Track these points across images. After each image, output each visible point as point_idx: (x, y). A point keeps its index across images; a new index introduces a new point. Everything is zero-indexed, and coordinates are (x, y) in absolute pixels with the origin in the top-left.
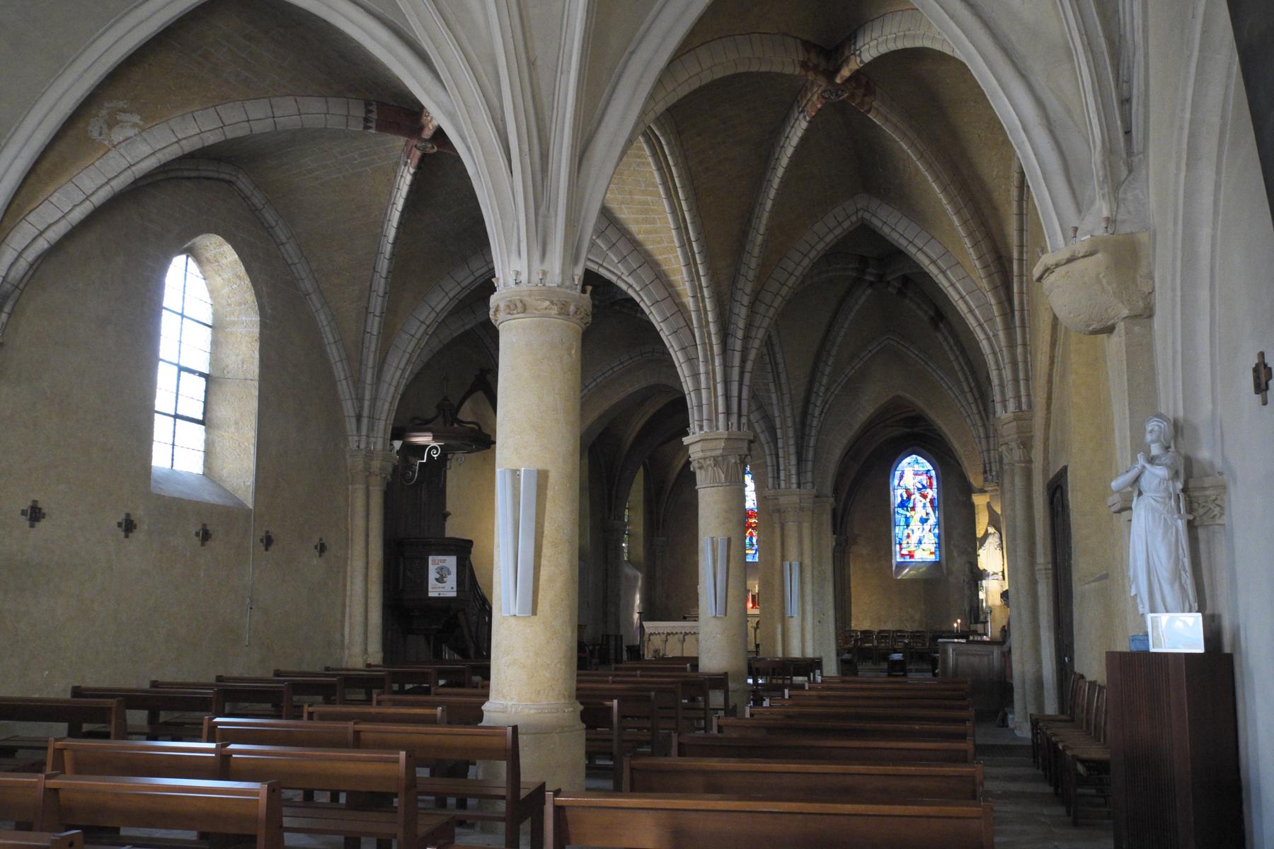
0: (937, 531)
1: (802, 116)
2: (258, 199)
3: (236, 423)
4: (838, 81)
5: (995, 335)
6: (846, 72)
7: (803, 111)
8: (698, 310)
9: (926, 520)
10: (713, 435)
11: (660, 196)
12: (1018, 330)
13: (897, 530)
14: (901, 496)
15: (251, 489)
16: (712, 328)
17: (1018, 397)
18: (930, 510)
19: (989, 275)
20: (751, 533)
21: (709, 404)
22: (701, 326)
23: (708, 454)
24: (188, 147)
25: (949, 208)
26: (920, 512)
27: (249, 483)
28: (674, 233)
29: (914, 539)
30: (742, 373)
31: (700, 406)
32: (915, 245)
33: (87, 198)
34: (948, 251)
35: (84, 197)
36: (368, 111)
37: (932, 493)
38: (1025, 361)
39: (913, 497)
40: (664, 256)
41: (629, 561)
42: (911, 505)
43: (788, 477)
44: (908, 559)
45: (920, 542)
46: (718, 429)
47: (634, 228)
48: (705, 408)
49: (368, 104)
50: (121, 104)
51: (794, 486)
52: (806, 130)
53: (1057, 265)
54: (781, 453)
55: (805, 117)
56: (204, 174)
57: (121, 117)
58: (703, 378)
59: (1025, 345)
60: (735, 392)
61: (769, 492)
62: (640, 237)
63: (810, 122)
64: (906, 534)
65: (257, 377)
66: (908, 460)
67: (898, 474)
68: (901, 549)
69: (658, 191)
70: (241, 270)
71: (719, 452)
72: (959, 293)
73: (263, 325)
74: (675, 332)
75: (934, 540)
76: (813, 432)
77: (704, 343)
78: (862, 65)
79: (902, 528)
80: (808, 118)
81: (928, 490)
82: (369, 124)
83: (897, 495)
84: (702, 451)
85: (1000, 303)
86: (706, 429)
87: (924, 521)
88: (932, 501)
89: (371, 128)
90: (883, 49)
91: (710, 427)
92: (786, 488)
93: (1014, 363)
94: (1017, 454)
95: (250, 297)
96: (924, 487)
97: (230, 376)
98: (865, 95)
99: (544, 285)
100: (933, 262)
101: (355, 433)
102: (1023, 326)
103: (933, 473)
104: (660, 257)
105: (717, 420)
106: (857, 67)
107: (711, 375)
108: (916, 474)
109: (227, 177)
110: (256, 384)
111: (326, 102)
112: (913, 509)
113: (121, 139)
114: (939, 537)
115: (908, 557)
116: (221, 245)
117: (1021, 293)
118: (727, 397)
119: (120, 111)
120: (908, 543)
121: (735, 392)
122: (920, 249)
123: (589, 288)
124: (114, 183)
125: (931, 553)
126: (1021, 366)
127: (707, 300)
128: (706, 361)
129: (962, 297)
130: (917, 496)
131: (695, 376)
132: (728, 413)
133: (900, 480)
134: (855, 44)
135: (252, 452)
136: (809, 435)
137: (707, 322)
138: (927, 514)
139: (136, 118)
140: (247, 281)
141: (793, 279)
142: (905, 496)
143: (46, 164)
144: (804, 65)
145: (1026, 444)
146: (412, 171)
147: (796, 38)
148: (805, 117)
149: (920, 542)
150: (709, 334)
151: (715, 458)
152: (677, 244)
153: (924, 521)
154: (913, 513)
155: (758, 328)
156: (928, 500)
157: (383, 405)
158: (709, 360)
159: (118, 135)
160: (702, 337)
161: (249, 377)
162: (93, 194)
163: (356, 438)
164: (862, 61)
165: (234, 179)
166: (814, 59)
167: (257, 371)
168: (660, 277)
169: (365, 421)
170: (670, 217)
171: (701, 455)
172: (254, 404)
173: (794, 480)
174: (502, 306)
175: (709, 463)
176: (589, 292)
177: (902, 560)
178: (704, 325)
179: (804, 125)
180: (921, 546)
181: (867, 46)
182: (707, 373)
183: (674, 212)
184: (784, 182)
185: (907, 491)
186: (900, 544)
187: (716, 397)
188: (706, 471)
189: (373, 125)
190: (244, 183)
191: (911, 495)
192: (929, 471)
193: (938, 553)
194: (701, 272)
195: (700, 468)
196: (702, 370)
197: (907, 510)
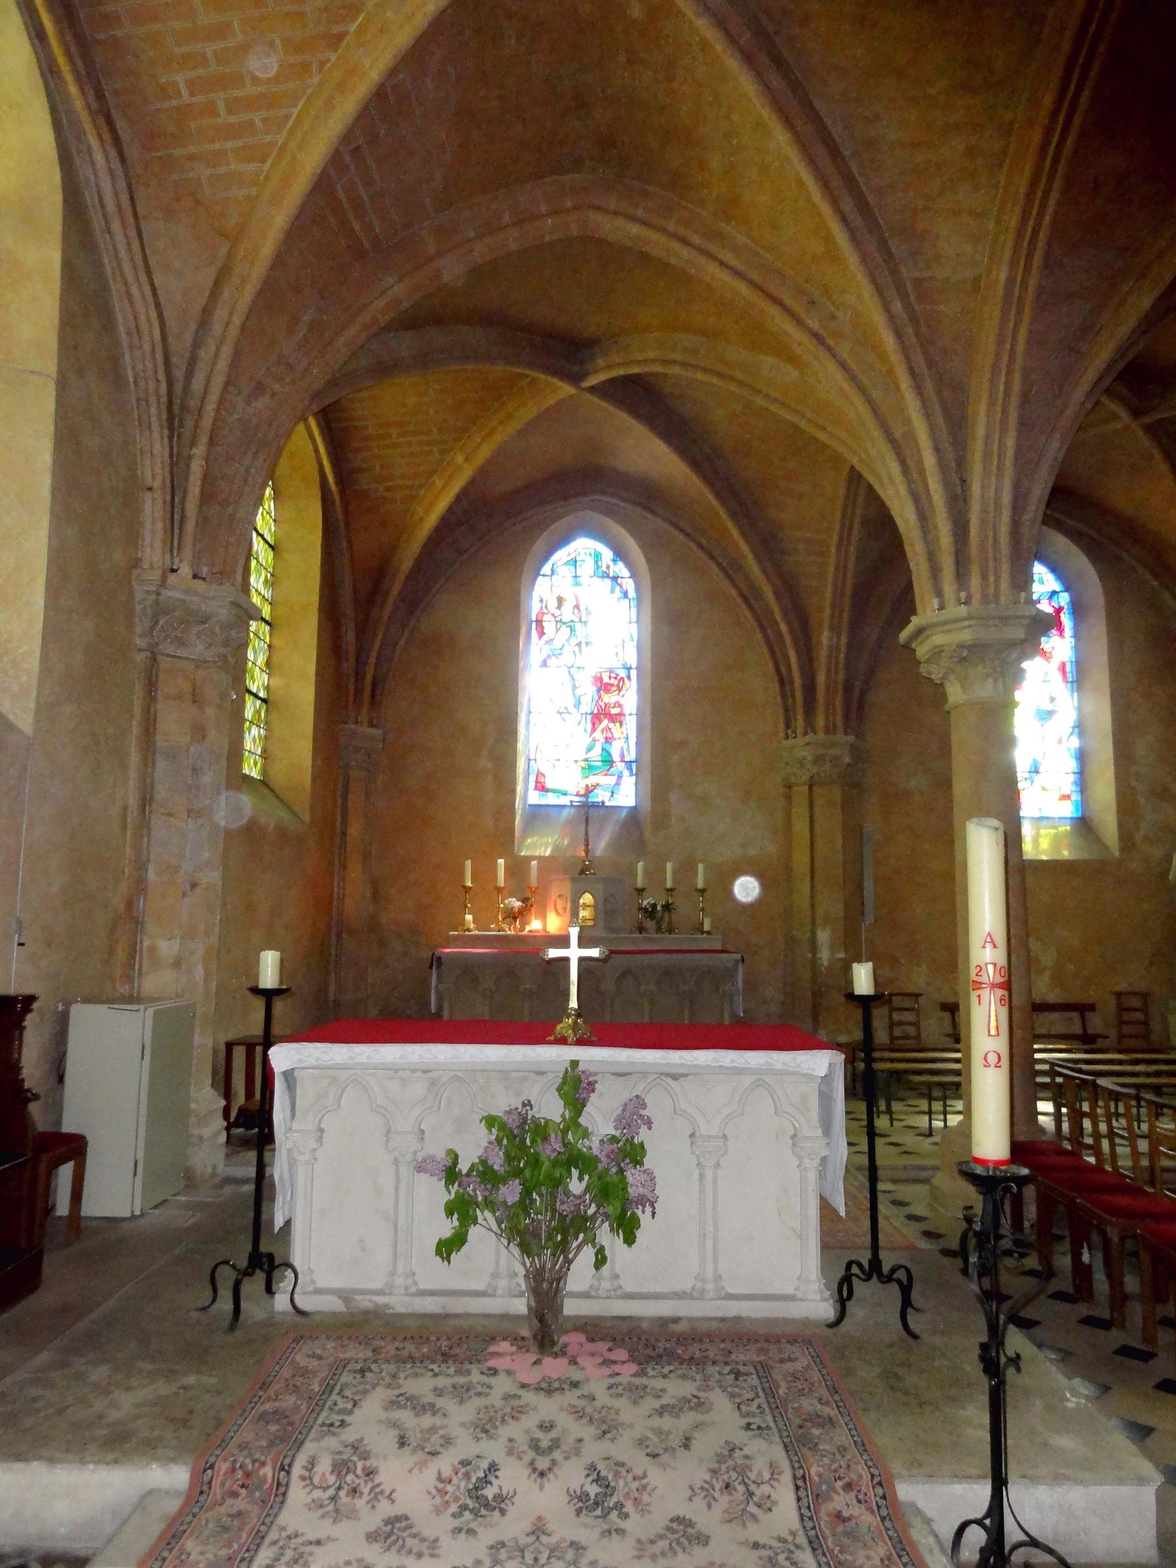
88: (1063, 667)
125: (1066, 797)
138: (1052, 700)
180: (1037, 778)
192: (1054, 593)
193: (1076, 797)
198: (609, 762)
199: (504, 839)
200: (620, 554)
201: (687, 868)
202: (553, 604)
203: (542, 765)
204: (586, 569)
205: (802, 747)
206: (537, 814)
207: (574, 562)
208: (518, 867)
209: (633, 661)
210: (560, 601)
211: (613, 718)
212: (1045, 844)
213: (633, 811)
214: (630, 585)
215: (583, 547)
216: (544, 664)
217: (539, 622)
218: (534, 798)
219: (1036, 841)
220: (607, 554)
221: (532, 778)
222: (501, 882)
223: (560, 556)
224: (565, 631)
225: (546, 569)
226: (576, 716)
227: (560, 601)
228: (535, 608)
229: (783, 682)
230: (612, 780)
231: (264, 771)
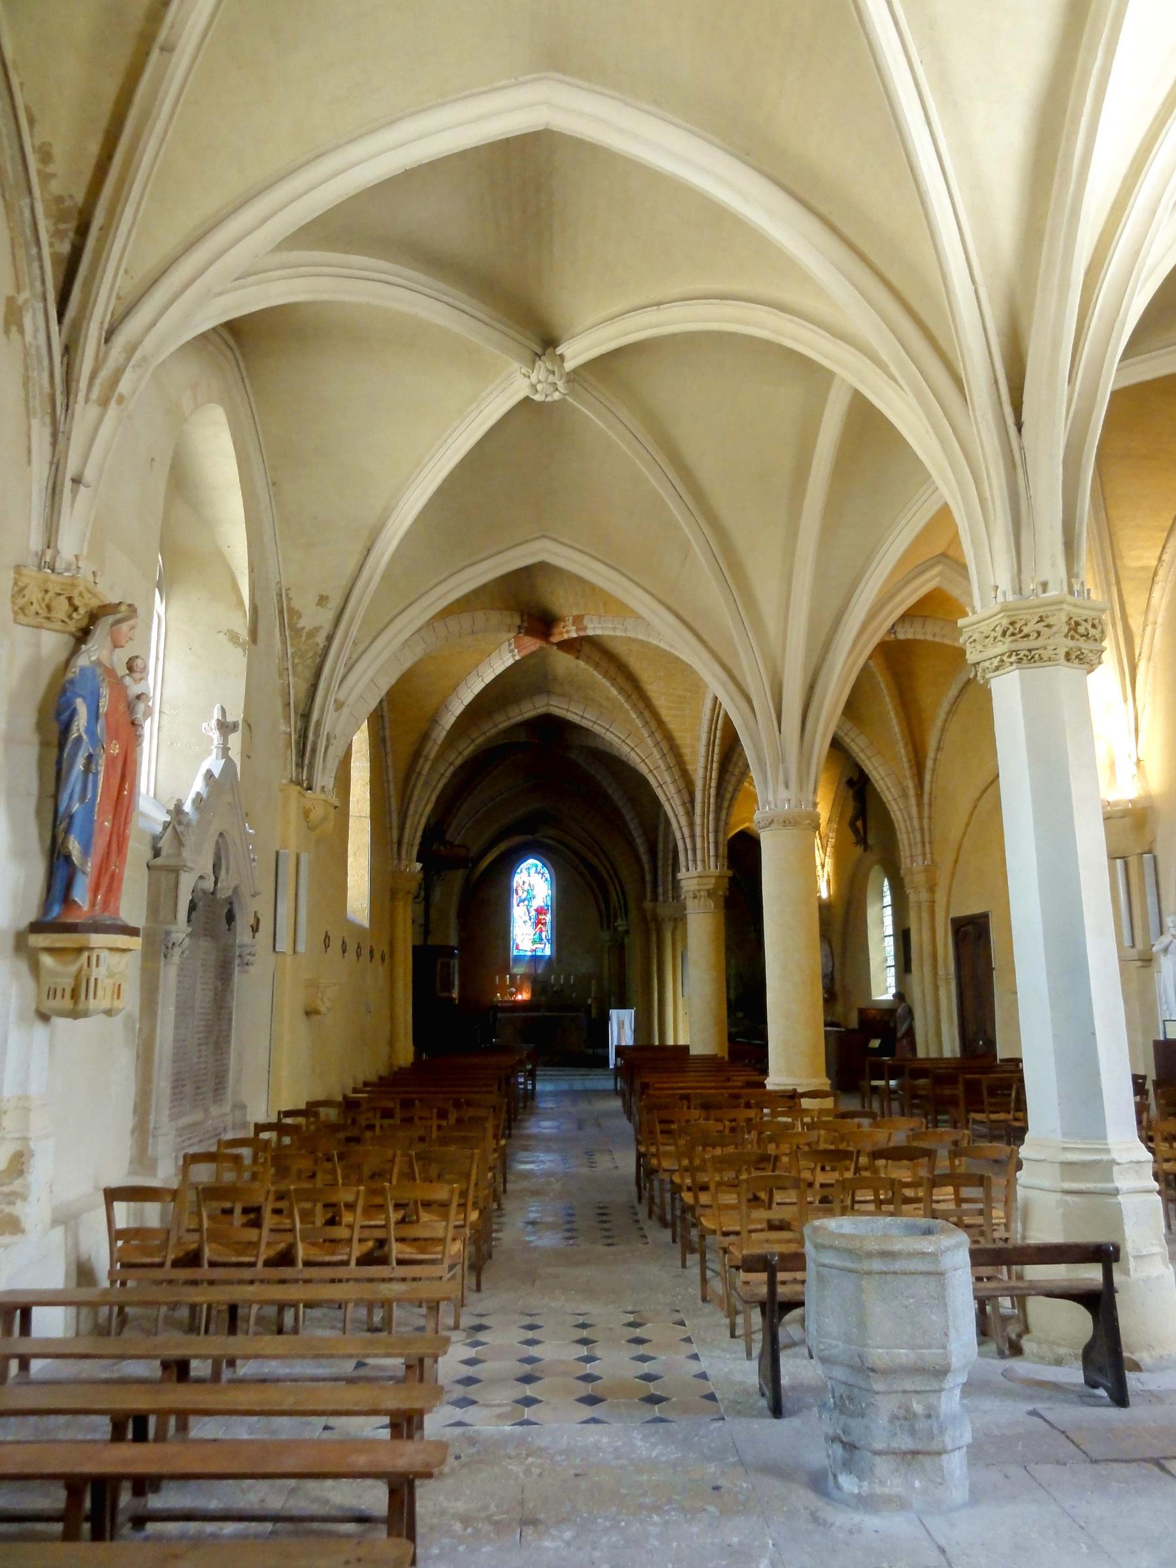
5: (907, 808)
10: (707, 873)
12: (926, 807)
15: (367, 911)
17: (924, 854)
19: (911, 768)
20: (541, 929)
21: (703, 848)
23: (702, 887)
36: (522, 621)
38: (930, 830)
43: (665, 892)
46: (709, 868)
49: (522, 616)
51: (671, 899)
59: (930, 818)
65: (368, 815)
71: (711, 886)
85: (915, 788)
91: (704, 867)
93: (922, 830)
94: (924, 896)
100: (862, 750)
101: (395, 856)
102: (930, 805)
110: (369, 821)
117: (932, 782)
126: (927, 833)
131: (691, 825)
137: (710, 787)
145: (932, 889)
146: (517, 658)
151: (708, 890)
161: (363, 815)
163: (396, 862)
169: (404, 848)
171: (697, 887)
182: (703, 825)
187: (709, 843)
189: (523, 631)
198: (542, 939)
199: (506, 968)
200: (544, 865)
201: (567, 979)
202: (521, 884)
203: (518, 941)
204: (533, 870)
205: (605, 936)
206: (518, 959)
207: (528, 869)
208: (513, 977)
209: (549, 903)
210: (524, 883)
211: (542, 924)
213: (550, 957)
214: (547, 876)
215: (531, 861)
216: (518, 905)
218: (515, 953)
220: (540, 865)
222: (508, 983)
223: (524, 866)
224: (525, 894)
225: (519, 871)
226: (529, 923)
227: (524, 883)
228: (515, 885)
229: (600, 911)
230: (542, 946)
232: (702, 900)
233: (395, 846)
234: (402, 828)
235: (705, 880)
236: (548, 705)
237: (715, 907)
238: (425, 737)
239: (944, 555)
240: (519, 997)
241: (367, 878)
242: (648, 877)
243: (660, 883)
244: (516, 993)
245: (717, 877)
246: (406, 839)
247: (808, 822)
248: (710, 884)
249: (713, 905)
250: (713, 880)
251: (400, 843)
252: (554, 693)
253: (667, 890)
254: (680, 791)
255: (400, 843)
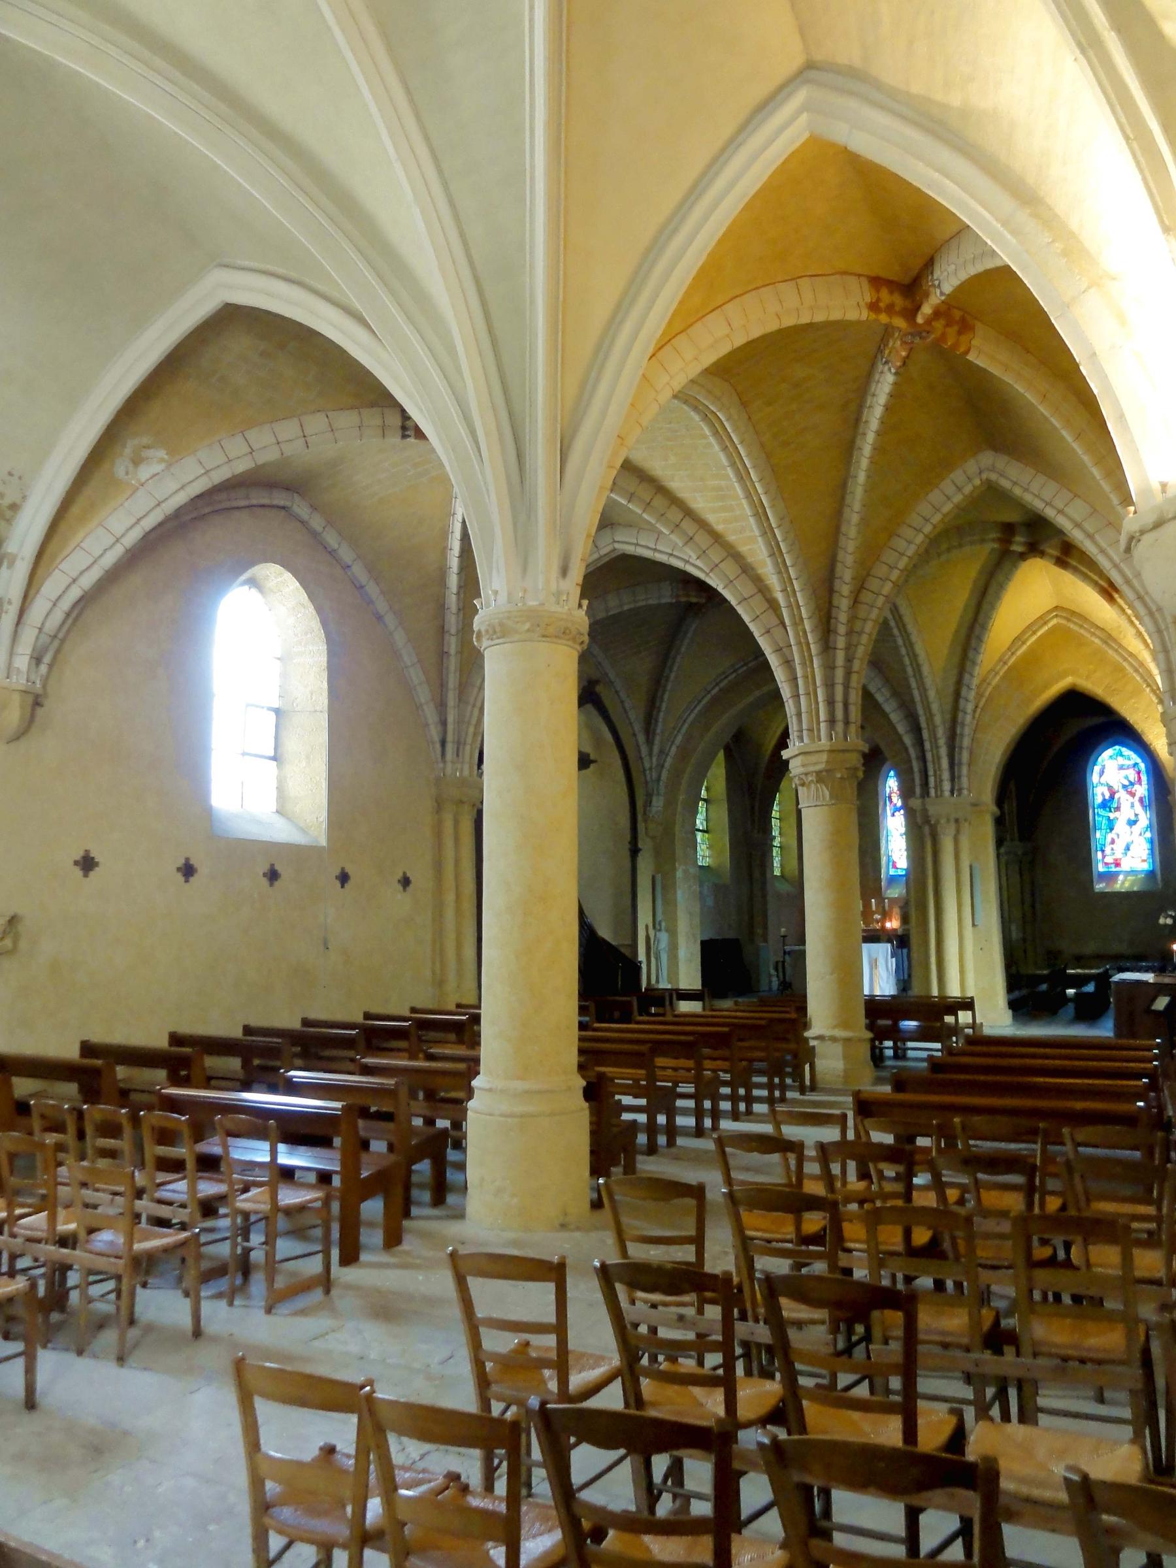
0: (1148, 835)
1: (886, 368)
2: (317, 522)
3: (308, 757)
4: (920, 320)
6: (927, 309)
7: (886, 363)
8: (789, 606)
9: (1135, 822)
10: (813, 748)
11: (731, 480)
13: (1098, 834)
14: (1103, 795)
15: (324, 826)
16: (808, 626)
18: (1138, 808)
21: (809, 712)
22: (795, 624)
23: (811, 769)
24: (218, 477)
25: (1086, 459)
26: (1126, 813)
27: (321, 819)
28: (752, 520)
29: (1119, 847)
30: (848, 673)
31: (799, 715)
32: (1053, 507)
33: (117, 540)
34: (1095, 510)
35: (113, 540)
37: (1142, 790)
39: (1116, 796)
40: (749, 547)
41: (782, 876)
42: (1115, 805)
44: (1113, 869)
45: (1128, 848)
46: (820, 740)
47: (711, 518)
48: (804, 716)
50: (145, 440)
51: (947, 794)
52: (895, 384)
53: (1143, 532)
54: (929, 756)
55: (890, 369)
56: (254, 502)
57: (146, 453)
58: (800, 682)
60: (839, 696)
61: (916, 803)
62: (719, 527)
63: (896, 374)
64: (1109, 840)
66: (1109, 752)
67: (1097, 769)
68: (1104, 857)
69: (728, 475)
70: (303, 596)
72: (1111, 560)
73: (331, 654)
74: (768, 632)
75: (1147, 846)
76: (967, 731)
77: (799, 643)
78: (943, 298)
79: (1104, 831)
80: (893, 370)
81: (1137, 787)
82: (408, 433)
83: (1098, 793)
84: (803, 766)
86: (806, 740)
87: (1132, 823)
88: (1141, 800)
89: (409, 436)
90: (963, 276)
91: (812, 739)
92: (937, 796)
95: (315, 623)
96: (1132, 784)
97: (299, 708)
98: (960, 333)
99: (524, 604)
100: (1078, 525)
101: (440, 759)
103: (1142, 766)
104: (743, 549)
105: (819, 730)
106: (939, 302)
107: (810, 679)
108: (1121, 768)
109: (282, 503)
111: (360, 413)
112: (1118, 809)
113: (148, 476)
114: (1151, 841)
115: (1113, 866)
116: (281, 574)
118: (831, 702)
119: (144, 447)
120: (1112, 849)
121: (839, 696)
122: (1060, 512)
123: (585, 603)
124: (142, 523)
125: (1144, 861)
127: (798, 594)
128: (803, 664)
129: (1116, 566)
130: (1122, 795)
131: (794, 680)
132: (832, 721)
133: (1101, 776)
134: (932, 273)
135: (324, 786)
136: (962, 735)
137: (802, 619)
138: (1136, 815)
139: (162, 453)
140: (311, 608)
141: (905, 560)
142: (1107, 796)
143: (75, 510)
144: (874, 307)
147: (859, 275)
148: (890, 369)
149: (1128, 848)
150: (805, 632)
151: (818, 773)
152: (757, 533)
153: (1132, 823)
154: (1117, 814)
155: (865, 620)
156: (1137, 798)
157: (468, 728)
158: (807, 662)
159: (145, 472)
160: (797, 635)
161: (318, 708)
162: (123, 535)
163: (441, 765)
164: (942, 294)
165: (288, 504)
166: (885, 296)
167: (326, 702)
168: (747, 569)
169: (450, 748)
170: (744, 502)
171: (802, 770)
172: (324, 737)
173: (947, 786)
174: (483, 630)
175: (810, 779)
176: (585, 608)
177: (1106, 870)
178: (798, 622)
179: (890, 378)
180: (1129, 853)
181: (946, 273)
182: (805, 677)
183: (748, 496)
184: (878, 449)
185: (1110, 788)
186: (1103, 851)
187: (817, 703)
188: (809, 787)
190: (301, 508)
191: (1114, 793)
192: (1135, 765)
194: (788, 563)
195: (803, 785)
196: (799, 673)
197: (1111, 811)
206: (892, 880)
212: (1127, 884)
217: (890, 797)
218: (892, 872)
219: (1123, 883)
221: (891, 864)
231: (782, 872)
232: (813, 785)
233: (438, 746)
234: (444, 723)
235: (813, 758)
236: (615, 541)
237: (831, 797)
238: (442, 607)
239: (810, 66)
240: (888, 925)
241: (324, 785)
242: (916, 766)
243: (931, 772)
244: (883, 920)
245: (831, 751)
246: (450, 737)
247: (527, 626)
248: (820, 762)
249: (827, 793)
250: (824, 757)
251: (443, 743)
252: (619, 524)
253: (941, 781)
254: (768, 632)
255: (443, 743)
